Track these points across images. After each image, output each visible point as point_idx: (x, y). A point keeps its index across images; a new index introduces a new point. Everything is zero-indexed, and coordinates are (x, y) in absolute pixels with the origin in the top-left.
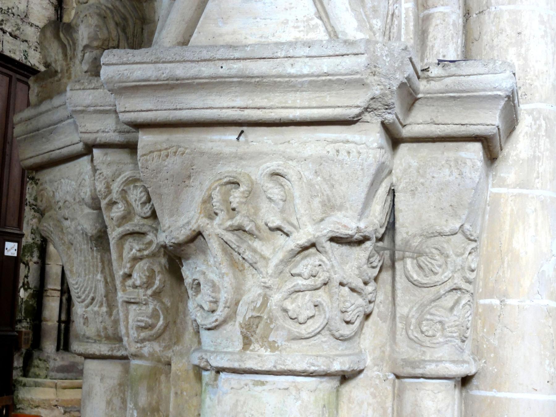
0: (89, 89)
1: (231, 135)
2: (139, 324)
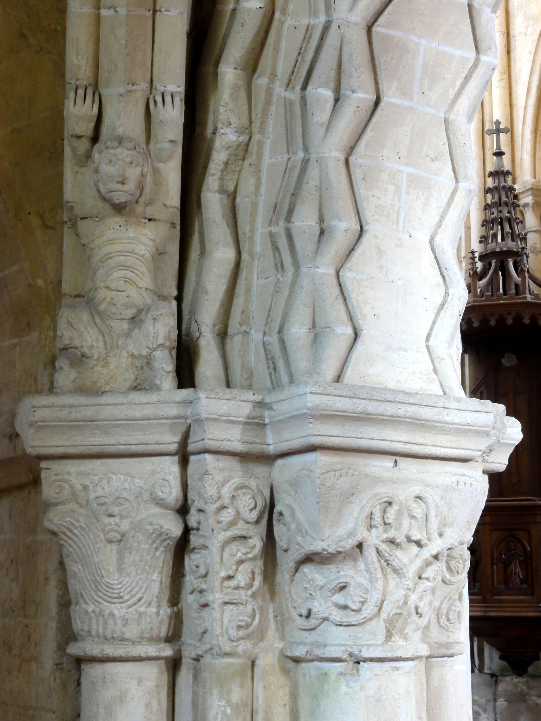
0: (224, 399)
1: (388, 463)
2: (240, 623)
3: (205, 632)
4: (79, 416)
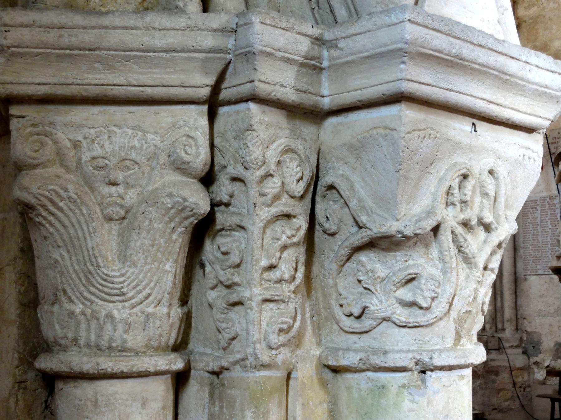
0: (280, 28)
2: (282, 326)
3: (233, 339)
4: (74, 41)
